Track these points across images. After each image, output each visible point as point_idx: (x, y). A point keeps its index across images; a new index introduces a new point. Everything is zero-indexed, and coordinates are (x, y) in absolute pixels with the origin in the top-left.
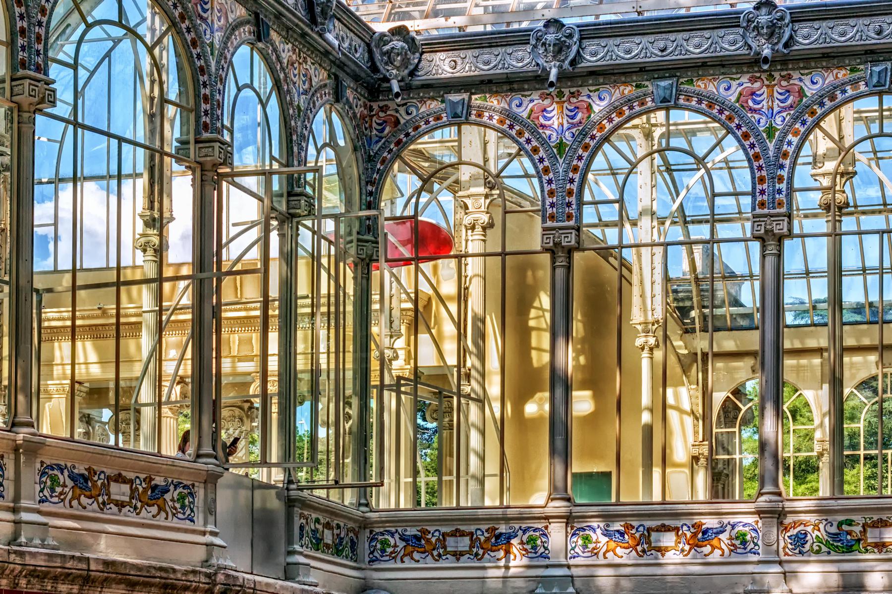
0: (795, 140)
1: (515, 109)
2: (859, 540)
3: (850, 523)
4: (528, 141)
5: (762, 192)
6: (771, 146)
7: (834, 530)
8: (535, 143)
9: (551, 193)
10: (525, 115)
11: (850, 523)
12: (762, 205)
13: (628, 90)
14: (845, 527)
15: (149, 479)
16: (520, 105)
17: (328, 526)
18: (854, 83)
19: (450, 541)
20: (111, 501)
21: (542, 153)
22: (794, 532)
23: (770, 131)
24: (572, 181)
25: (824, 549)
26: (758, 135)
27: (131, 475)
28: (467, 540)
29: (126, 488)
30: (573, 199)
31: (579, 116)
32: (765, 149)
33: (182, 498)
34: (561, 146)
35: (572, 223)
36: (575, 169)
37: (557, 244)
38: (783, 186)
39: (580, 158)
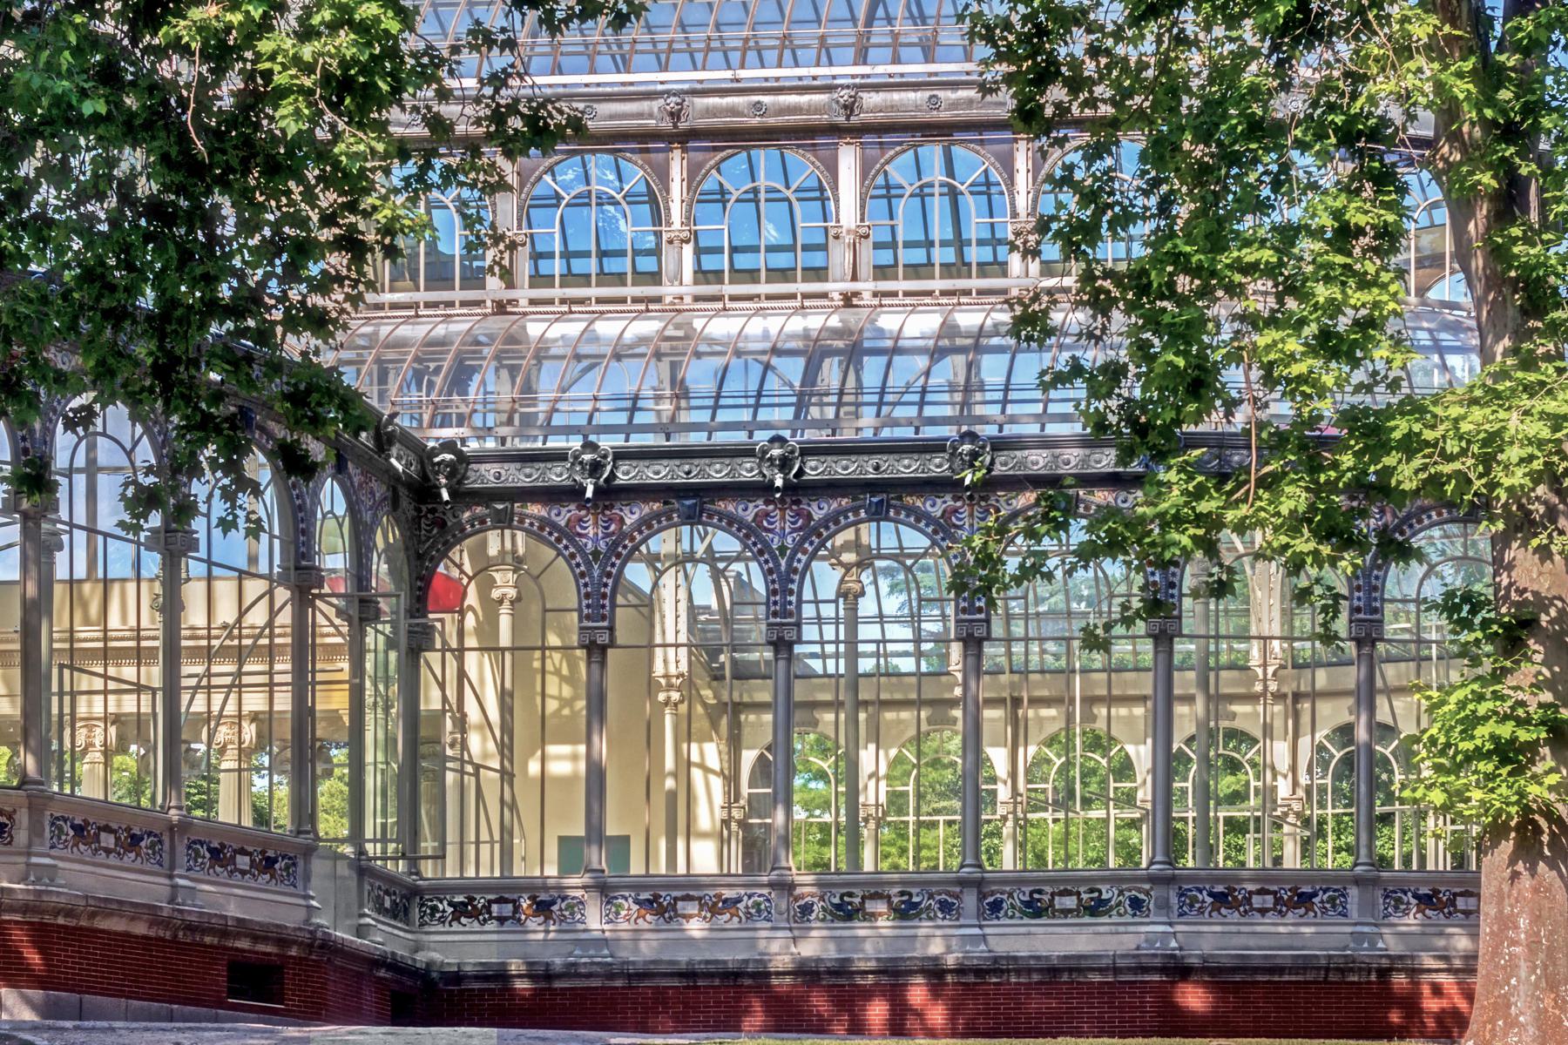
0: (804, 558)
1: (554, 518)
2: (858, 910)
4: (566, 547)
5: (775, 603)
6: (783, 562)
7: (1027, 898)
8: (572, 550)
9: (587, 596)
10: (563, 523)
11: (850, 895)
12: (775, 614)
13: (656, 506)
14: (1036, 896)
15: (263, 852)
16: (558, 514)
17: (387, 893)
18: (856, 511)
19: (495, 907)
20: (237, 870)
21: (578, 559)
22: (991, 899)
23: (783, 549)
24: (606, 585)
26: (771, 553)
27: (250, 849)
28: (510, 906)
29: (247, 859)
30: (607, 602)
31: (613, 527)
32: (778, 565)
33: (287, 868)
34: (596, 553)
35: (605, 624)
36: (609, 575)
37: (593, 643)
38: (793, 599)
39: (613, 565)
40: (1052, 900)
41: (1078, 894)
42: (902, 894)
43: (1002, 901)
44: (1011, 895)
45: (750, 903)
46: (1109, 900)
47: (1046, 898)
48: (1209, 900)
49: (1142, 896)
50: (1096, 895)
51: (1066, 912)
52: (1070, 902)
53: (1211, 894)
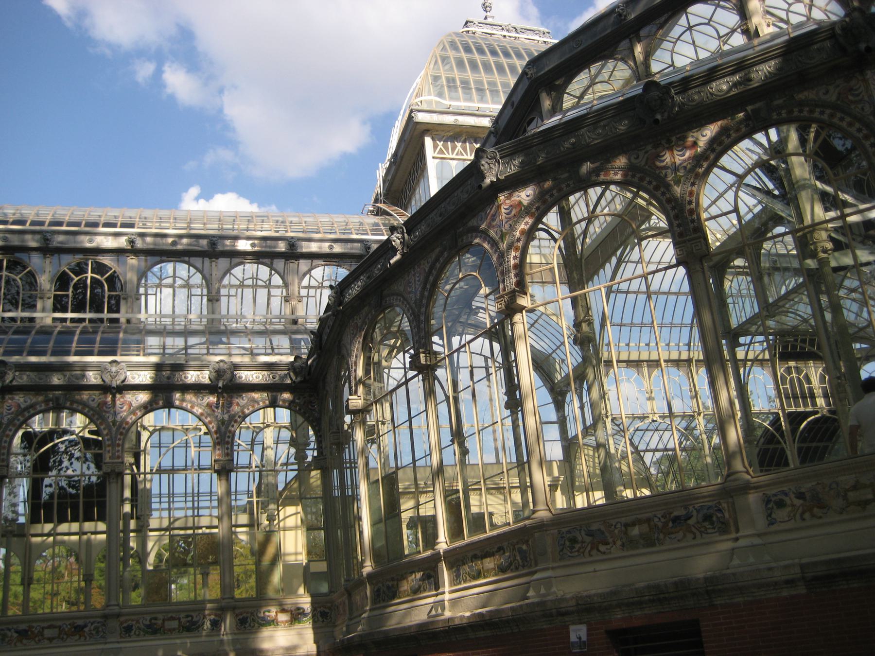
3: (156, 619)
7: (148, 623)
14: (153, 621)
25: (142, 633)
40: (163, 623)
41: (179, 619)
42: (187, 616)
43: (132, 626)
44: (138, 622)
45: (92, 628)
46: (198, 622)
47: (160, 622)
48: (15, 635)
49: (327, 610)
50: (190, 618)
51: (171, 630)
52: (174, 624)
53: (16, 632)
